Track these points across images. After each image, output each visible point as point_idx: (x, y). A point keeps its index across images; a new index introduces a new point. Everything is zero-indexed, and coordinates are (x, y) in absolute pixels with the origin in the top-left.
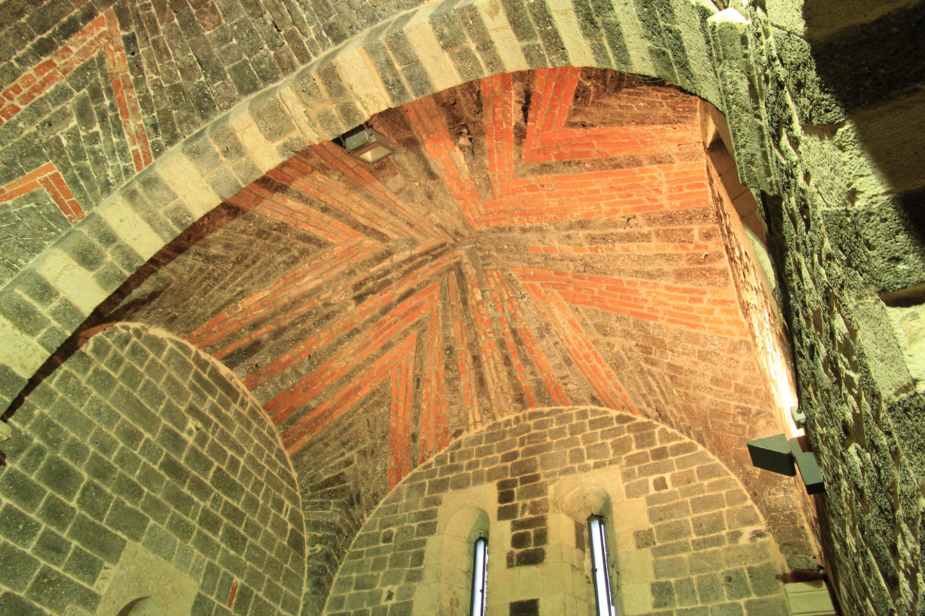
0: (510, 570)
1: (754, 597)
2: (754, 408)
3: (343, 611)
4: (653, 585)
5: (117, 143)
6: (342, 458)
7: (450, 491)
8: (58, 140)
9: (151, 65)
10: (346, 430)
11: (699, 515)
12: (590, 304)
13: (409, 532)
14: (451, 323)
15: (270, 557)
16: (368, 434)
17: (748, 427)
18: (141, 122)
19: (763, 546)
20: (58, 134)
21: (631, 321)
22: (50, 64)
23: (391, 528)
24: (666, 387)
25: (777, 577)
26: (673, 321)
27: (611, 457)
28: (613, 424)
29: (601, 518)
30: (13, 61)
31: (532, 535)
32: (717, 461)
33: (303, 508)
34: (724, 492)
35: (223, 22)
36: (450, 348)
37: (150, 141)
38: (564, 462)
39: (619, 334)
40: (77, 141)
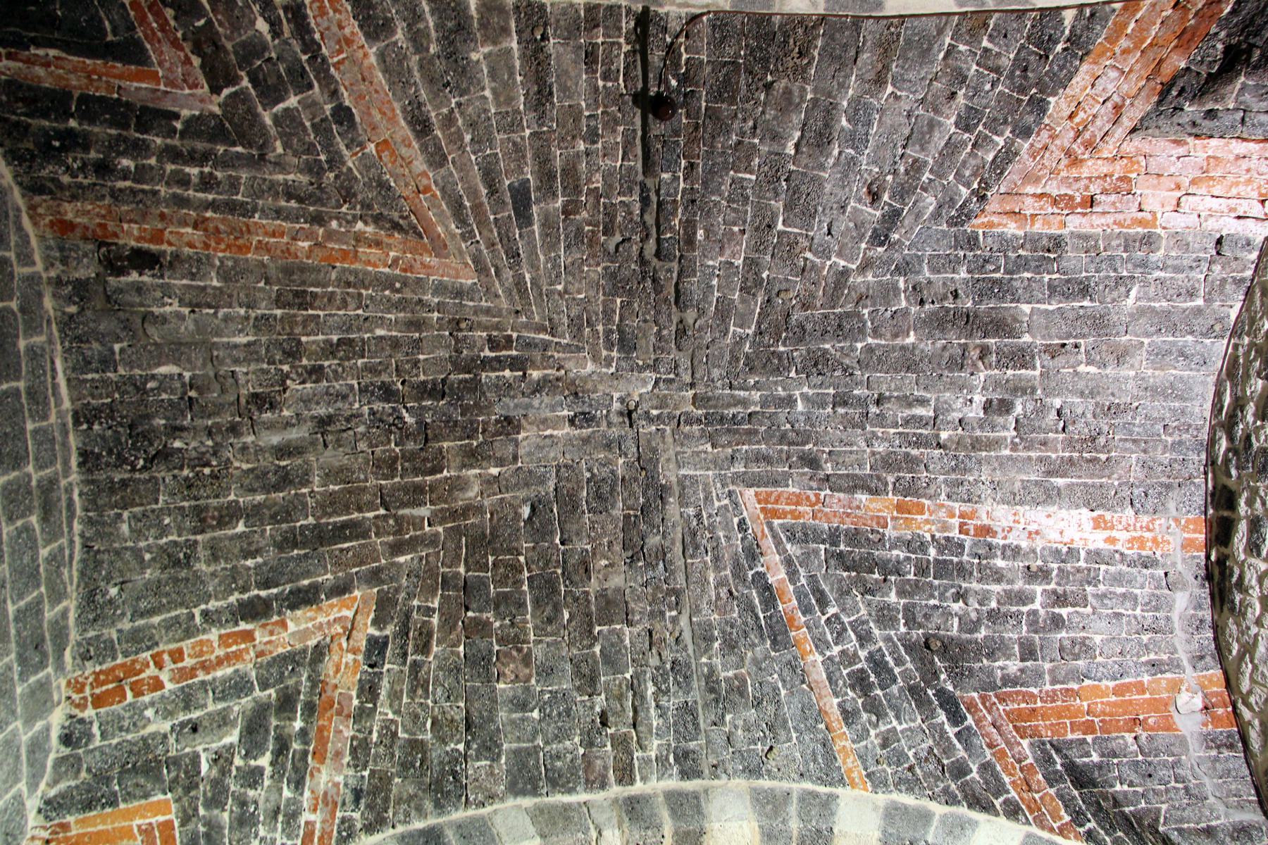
5: (288, 800)
8: (195, 759)
9: (395, 696)
18: (340, 779)
20: (199, 749)
22: (248, 636)
30: (197, 612)
35: (533, 681)
37: (339, 814)
40: (224, 772)
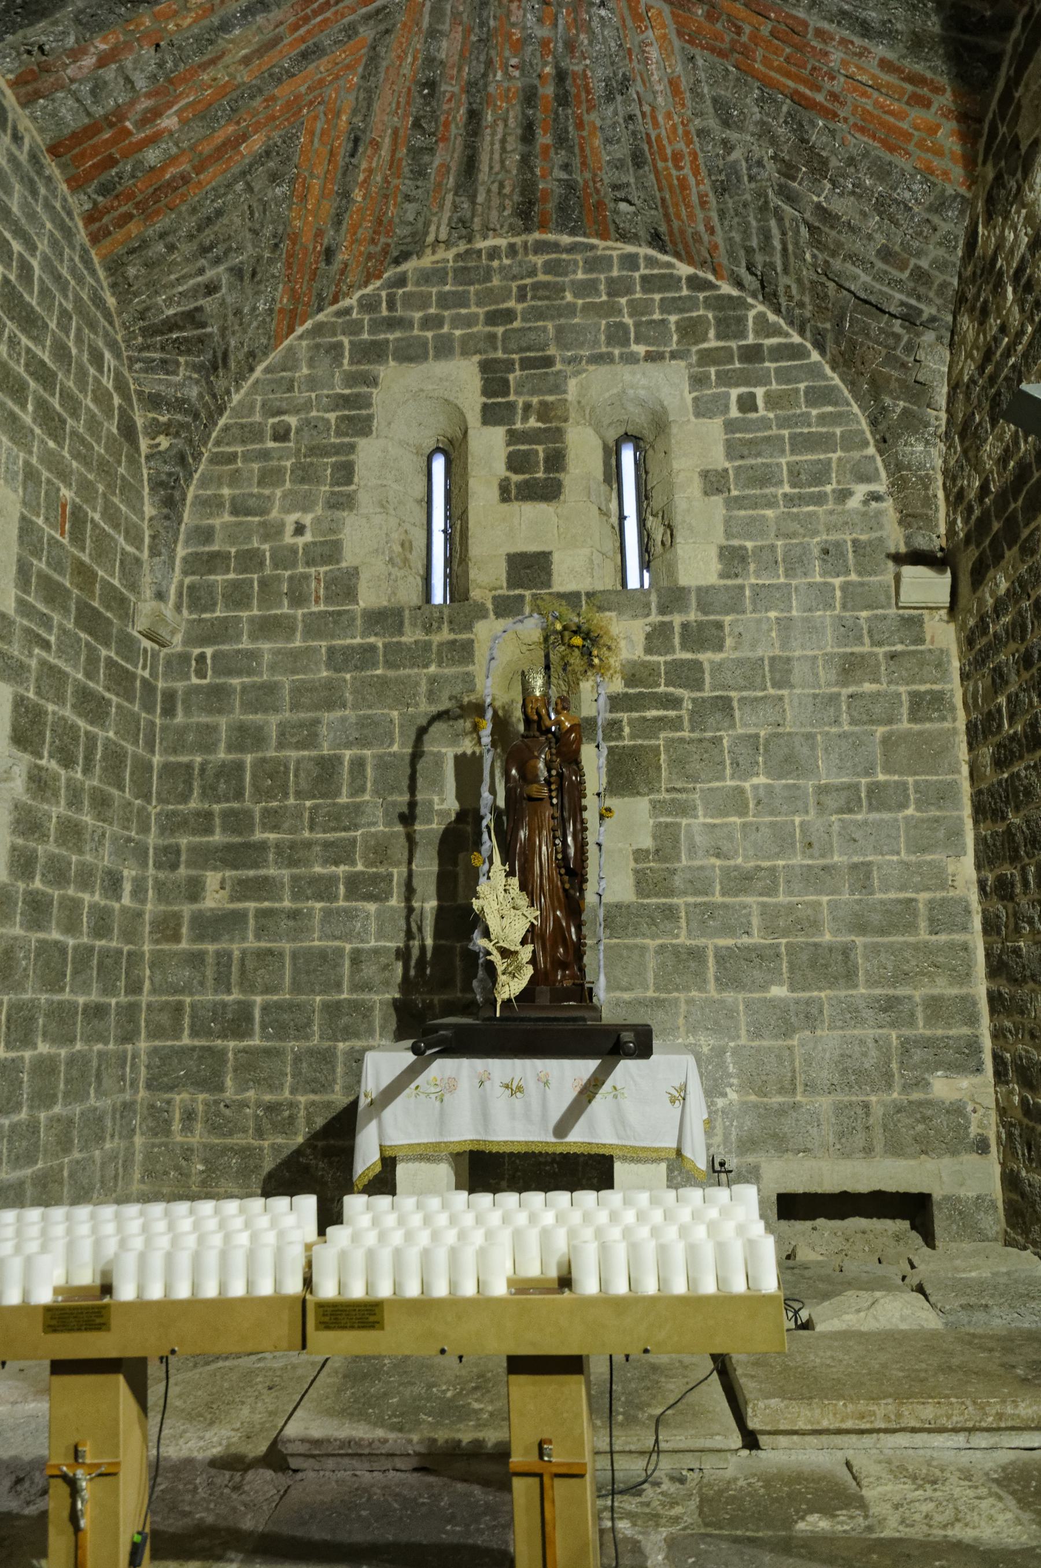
0: (505, 506)
1: (854, 577)
2: (928, 311)
3: (215, 548)
4: (722, 548)
6: (200, 279)
7: (392, 363)
10: (209, 221)
11: (798, 458)
12: (722, 54)
13: (320, 425)
14: (446, 27)
15: (99, 455)
16: (249, 236)
17: (905, 339)
19: (879, 513)
21: (785, 109)
23: (285, 418)
24: (796, 244)
25: (889, 556)
26: (862, 130)
27: (674, 347)
28: (680, 289)
29: (636, 440)
31: (541, 455)
32: (837, 381)
33: (130, 368)
34: (838, 431)
36: (431, 84)
38: (596, 342)
39: (752, 128)
